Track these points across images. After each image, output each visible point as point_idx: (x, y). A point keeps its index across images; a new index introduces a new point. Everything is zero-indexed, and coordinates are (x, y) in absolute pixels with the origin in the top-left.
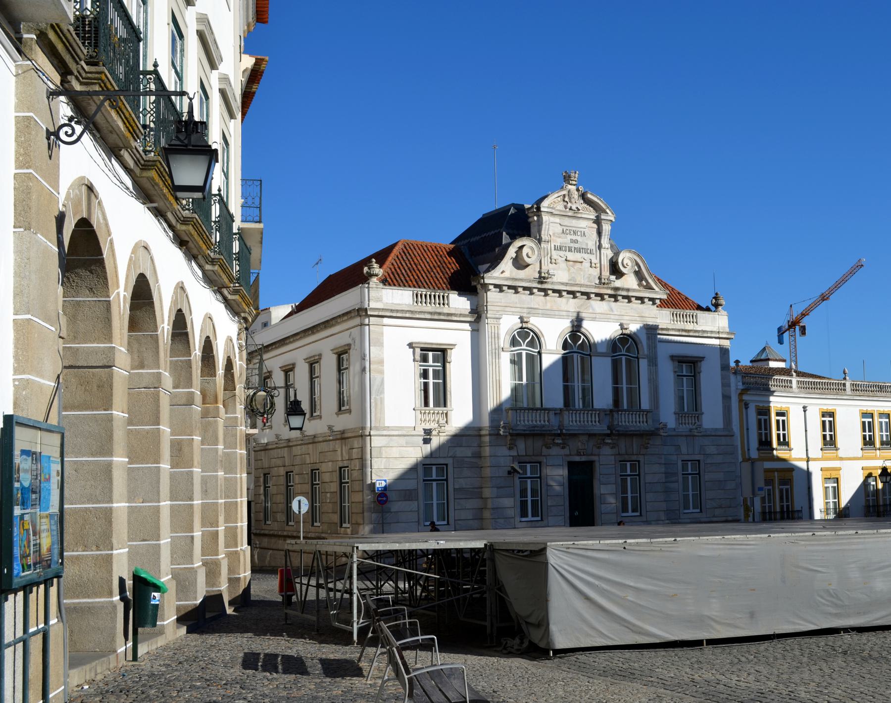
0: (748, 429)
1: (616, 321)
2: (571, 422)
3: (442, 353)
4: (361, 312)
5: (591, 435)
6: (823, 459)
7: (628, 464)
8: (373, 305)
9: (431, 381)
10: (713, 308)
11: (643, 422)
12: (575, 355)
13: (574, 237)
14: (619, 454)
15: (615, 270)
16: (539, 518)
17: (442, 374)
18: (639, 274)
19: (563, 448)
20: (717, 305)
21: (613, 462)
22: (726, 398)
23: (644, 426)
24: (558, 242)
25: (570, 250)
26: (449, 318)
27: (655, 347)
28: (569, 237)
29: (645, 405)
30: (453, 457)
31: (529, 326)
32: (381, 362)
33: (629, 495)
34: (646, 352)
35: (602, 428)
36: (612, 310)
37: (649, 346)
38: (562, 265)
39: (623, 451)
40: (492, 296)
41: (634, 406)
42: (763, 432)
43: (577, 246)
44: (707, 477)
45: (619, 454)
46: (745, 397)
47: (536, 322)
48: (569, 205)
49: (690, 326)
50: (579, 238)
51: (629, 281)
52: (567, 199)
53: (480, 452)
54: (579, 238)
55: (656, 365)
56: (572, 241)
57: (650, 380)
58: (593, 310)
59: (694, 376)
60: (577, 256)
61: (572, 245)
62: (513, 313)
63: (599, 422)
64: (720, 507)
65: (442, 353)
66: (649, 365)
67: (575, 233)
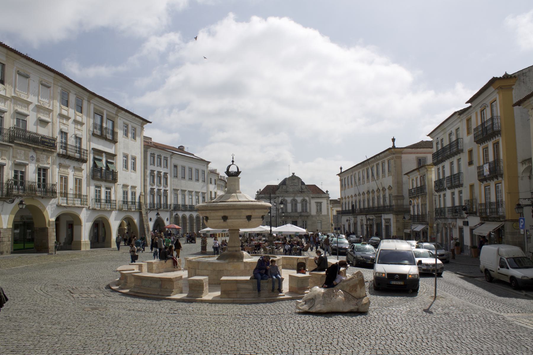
2: (292, 214)
5: (296, 217)
22: (328, 209)
24: (291, 185)
29: (308, 211)
41: (306, 211)
46: (333, 209)
49: (320, 197)
60: (295, 187)
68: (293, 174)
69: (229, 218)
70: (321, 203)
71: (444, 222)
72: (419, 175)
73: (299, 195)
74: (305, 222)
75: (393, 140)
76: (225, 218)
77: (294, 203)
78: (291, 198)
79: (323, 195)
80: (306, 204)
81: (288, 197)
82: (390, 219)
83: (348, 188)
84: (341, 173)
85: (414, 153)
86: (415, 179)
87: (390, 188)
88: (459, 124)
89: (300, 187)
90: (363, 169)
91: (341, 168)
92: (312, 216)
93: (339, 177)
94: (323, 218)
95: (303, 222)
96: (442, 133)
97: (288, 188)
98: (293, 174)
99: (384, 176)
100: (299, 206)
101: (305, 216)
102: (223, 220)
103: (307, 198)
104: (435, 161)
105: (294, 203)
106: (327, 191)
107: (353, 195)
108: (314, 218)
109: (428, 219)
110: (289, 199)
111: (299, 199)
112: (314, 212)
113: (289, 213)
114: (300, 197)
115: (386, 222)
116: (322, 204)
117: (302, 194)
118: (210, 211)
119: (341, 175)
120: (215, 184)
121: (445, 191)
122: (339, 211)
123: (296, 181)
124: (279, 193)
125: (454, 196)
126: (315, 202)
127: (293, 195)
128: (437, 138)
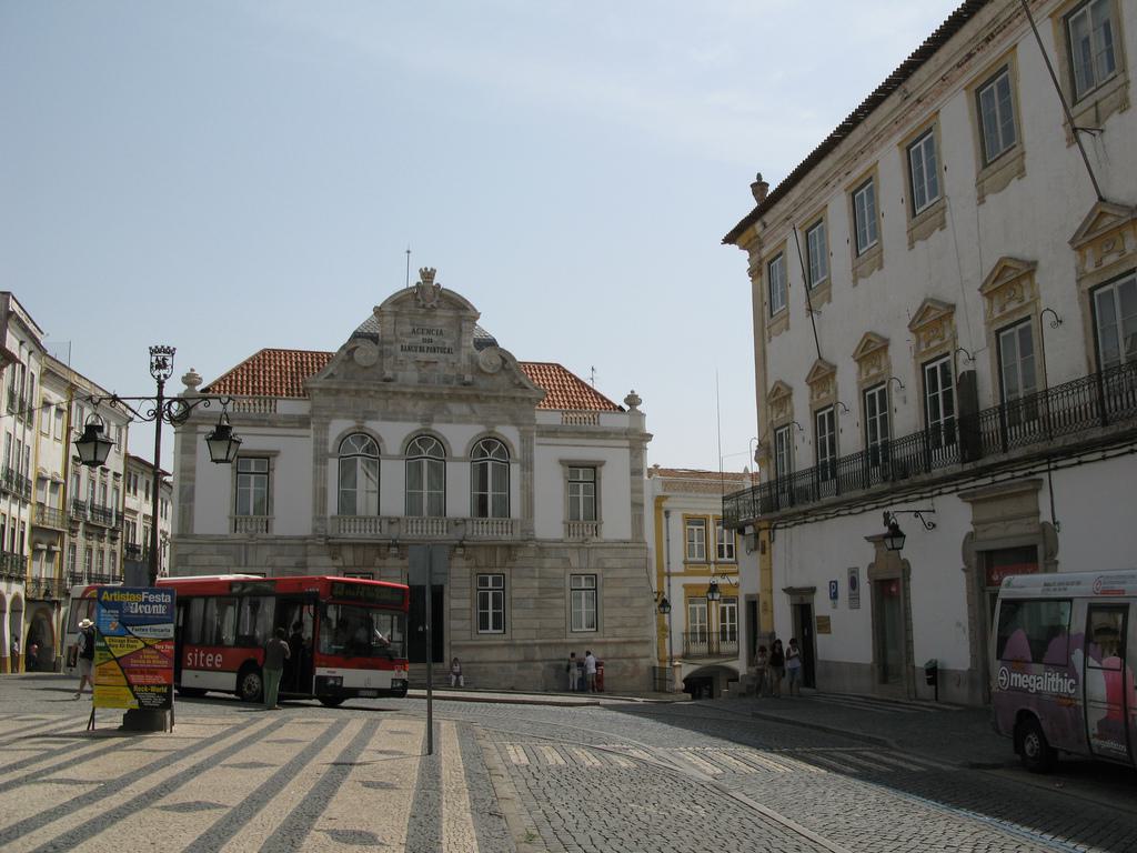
0: (668, 540)
1: (480, 423)
2: (410, 533)
6: (686, 574)
7: (490, 578)
10: (627, 408)
11: (502, 532)
12: (425, 461)
13: (427, 337)
14: (477, 566)
16: (502, 631)
19: (402, 559)
21: (468, 575)
22: (637, 506)
23: (506, 538)
24: (408, 341)
25: (422, 350)
27: (532, 451)
28: (421, 337)
30: (273, 566)
31: (367, 432)
33: (491, 611)
34: (518, 456)
35: (455, 536)
36: (474, 412)
37: (523, 451)
38: (413, 367)
39: (483, 563)
43: (430, 345)
44: (604, 593)
45: (477, 566)
46: (666, 504)
47: (375, 426)
48: (422, 303)
50: (434, 338)
52: (419, 297)
53: (305, 563)
54: (434, 338)
55: (532, 470)
56: (424, 340)
57: (522, 487)
58: (450, 412)
59: (595, 482)
60: (432, 356)
61: (422, 345)
63: (447, 531)
64: (623, 626)
66: (522, 470)
67: (429, 332)
68: (428, 275)
70: (594, 467)
73: (458, 408)
74: (497, 582)
77: (426, 452)
78: (416, 426)
80: (503, 473)
92: (543, 548)
94: (608, 565)
95: (484, 582)
97: (388, 361)
98: (428, 275)
101: (492, 547)
103: (510, 433)
105: (426, 452)
106: (633, 400)
108: (548, 563)
110: (393, 434)
111: (459, 435)
112: (549, 521)
113: (392, 521)
114: (464, 420)
117: (476, 406)
123: (443, 317)
126: (562, 462)
127: (421, 407)
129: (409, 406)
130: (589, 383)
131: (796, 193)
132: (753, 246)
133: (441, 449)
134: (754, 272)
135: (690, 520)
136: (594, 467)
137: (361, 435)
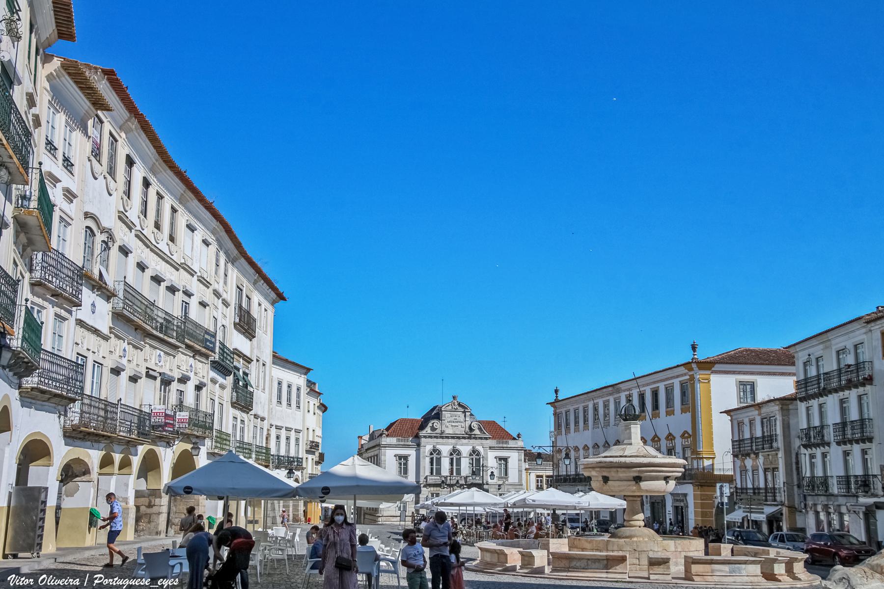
3: (406, 458)
4: (379, 445)
8: (383, 443)
9: (402, 466)
15: (471, 429)
17: (406, 464)
18: (480, 429)
20: (519, 437)
22: (520, 471)
26: (408, 446)
32: (385, 461)
40: (423, 440)
42: (539, 484)
47: (438, 447)
49: (505, 446)
51: (477, 432)
60: (456, 424)
62: (431, 444)
65: (406, 458)
69: (643, 479)
70: (505, 460)
71: (826, 503)
72: (760, 414)
75: (694, 348)
76: (638, 479)
79: (512, 444)
80: (478, 461)
81: (442, 445)
82: (685, 495)
83: (577, 430)
84: (557, 401)
85: (734, 373)
86: (746, 421)
87: (686, 435)
88: (865, 336)
89: (467, 426)
90: (618, 395)
91: (556, 391)
93: (552, 409)
96: (821, 346)
97: (444, 426)
99: (670, 412)
100: (465, 465)
102: (634, 483)
103: (480, 448)
104: (803, 394)
107: (590, 446)
109: (782, 497)
110: (445, 449)
111: (465, 449)
114: (467, 444)
115: (675, 500)
116: (510, 460)
118: (591, 469)
119: (556, 404)
120: (314, 414)
121: (827, 447)
122: (551, 476)
124: (425, 437)
125: (866, 457)
126: (496, 458)
128: (809, 355)
129: (451, 441)
130: (502, 425)
131: (564, 402)
132: (555, 407)
133: (459, 453)
134: (555, 414)
135: (538, 476)
136: (505, 460)
137: (435, 451)
